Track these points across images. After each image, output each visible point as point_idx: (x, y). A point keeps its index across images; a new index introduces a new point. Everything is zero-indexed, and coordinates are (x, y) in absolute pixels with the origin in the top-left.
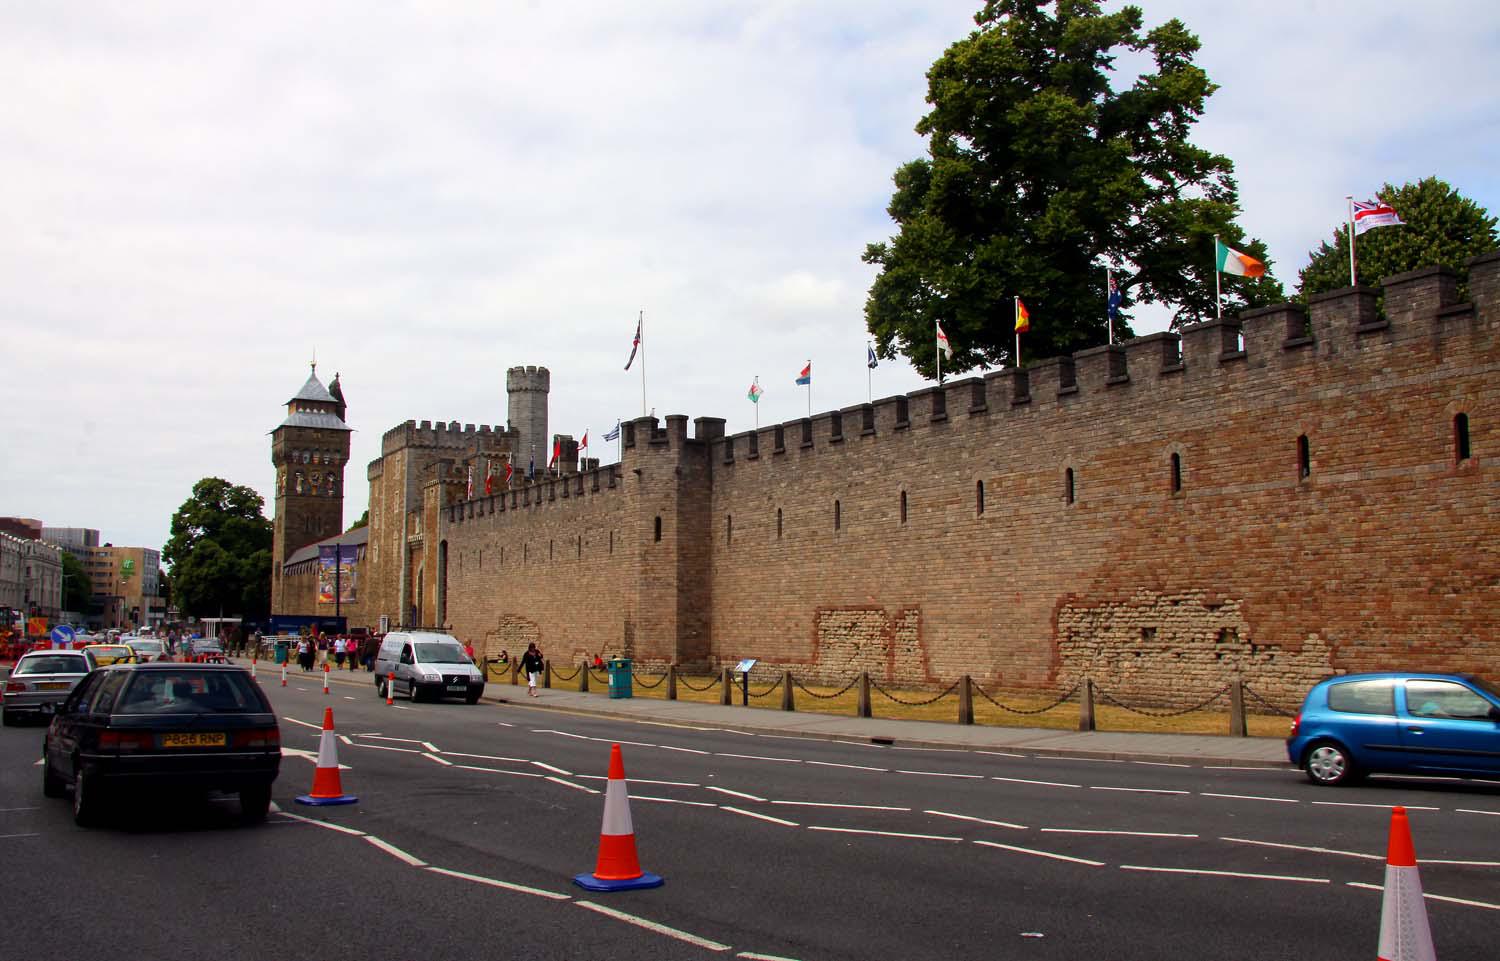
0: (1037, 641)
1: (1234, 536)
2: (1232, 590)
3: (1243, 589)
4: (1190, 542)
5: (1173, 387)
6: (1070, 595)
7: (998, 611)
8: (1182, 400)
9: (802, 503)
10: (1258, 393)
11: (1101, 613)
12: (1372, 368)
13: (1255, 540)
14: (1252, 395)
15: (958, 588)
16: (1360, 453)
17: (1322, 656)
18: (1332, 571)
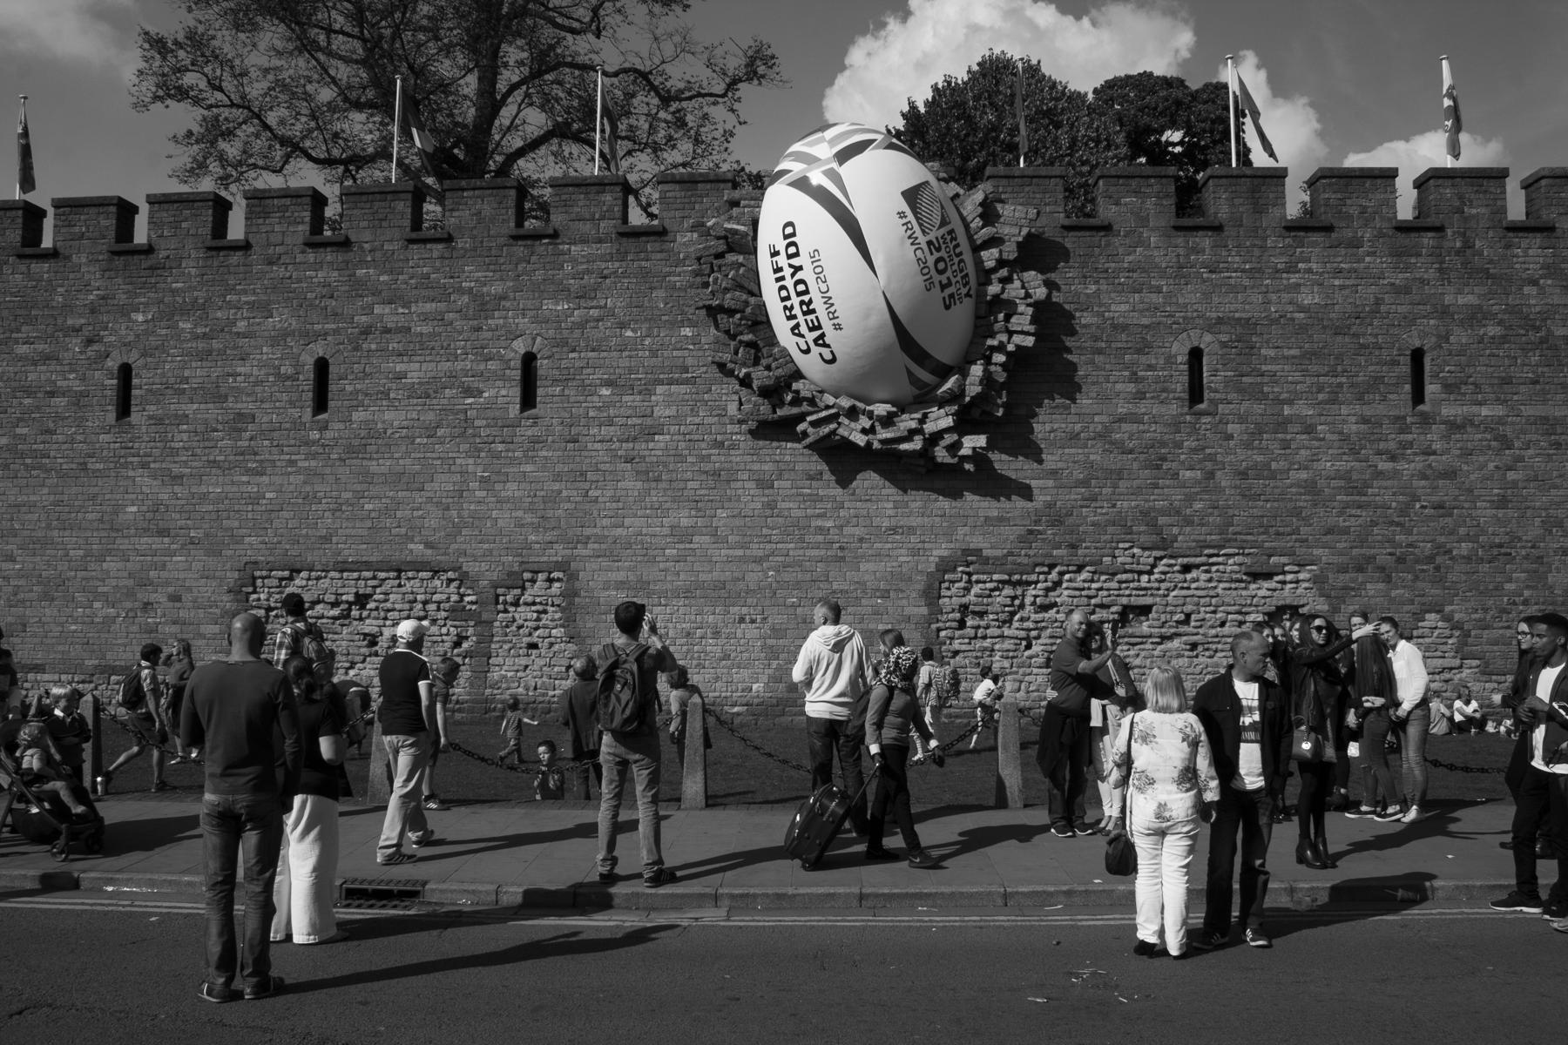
1: (1304, 475)
3: (1315, 552)
4: (1224, 479)
5: (1198, 251)
6: (967, 552)
7: (786, 577)
9: (205, 355)
10: (1348, 282)
11: (1037, 582)
12: (1524, 276)
13: (1342, 483)
14: (1337, 282)
15: (683, 535)
16: (1506, 381)
17: (1446, 643)
18: (1462, 531)
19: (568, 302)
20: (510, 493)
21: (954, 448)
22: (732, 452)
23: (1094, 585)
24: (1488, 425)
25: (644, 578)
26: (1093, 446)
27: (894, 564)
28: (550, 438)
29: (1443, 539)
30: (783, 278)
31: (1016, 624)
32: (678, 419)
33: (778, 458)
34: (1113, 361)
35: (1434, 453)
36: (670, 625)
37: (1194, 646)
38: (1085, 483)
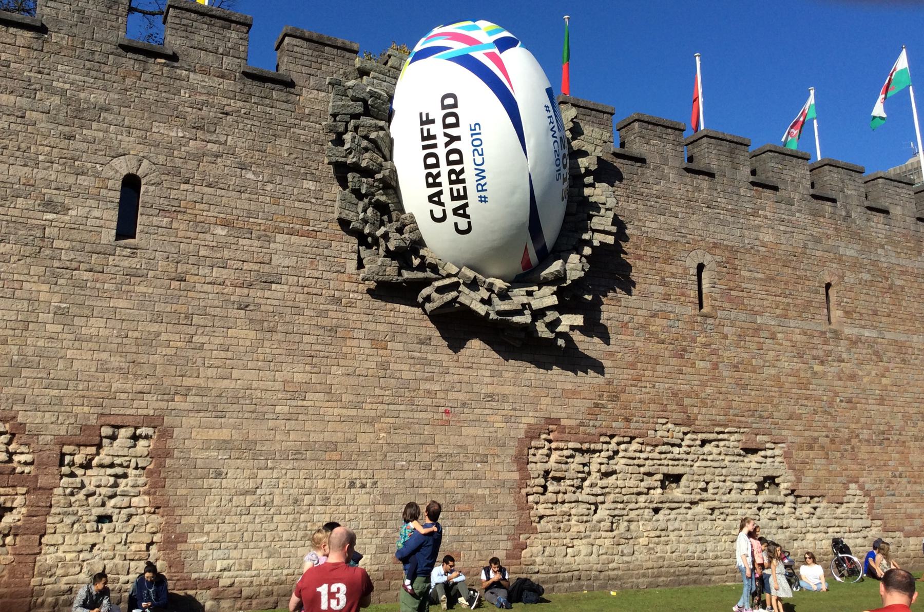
0: (487, 492)
1: (773, 371)
2: (774, 432)
3: (784, 433)
6: (550, 421)
7: (397, 439)
8: (708, 207)
11: (600, 451)
15: (299, 392)
17: (861, 508)
19: (183, 130)
20: (93, 331)
21: (552, 325)
22: (349, 309)
23: (643, 455)
24: (871, 343)
25: (251, 437)
26: (637, 335)
27: (492, 430)
28: (151, 274)
29: (853, 426)
30: (434, 146)
31: (587, 490)
32: (297, 271)
33: (392, 320)
34: (649, 267)
35: (843, 361)
36: (277, 491)
37: (713, 509)
38: (633, 365)
